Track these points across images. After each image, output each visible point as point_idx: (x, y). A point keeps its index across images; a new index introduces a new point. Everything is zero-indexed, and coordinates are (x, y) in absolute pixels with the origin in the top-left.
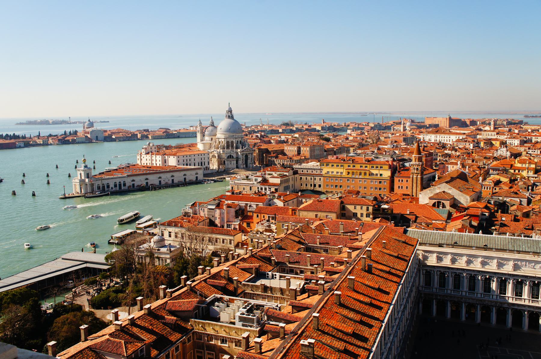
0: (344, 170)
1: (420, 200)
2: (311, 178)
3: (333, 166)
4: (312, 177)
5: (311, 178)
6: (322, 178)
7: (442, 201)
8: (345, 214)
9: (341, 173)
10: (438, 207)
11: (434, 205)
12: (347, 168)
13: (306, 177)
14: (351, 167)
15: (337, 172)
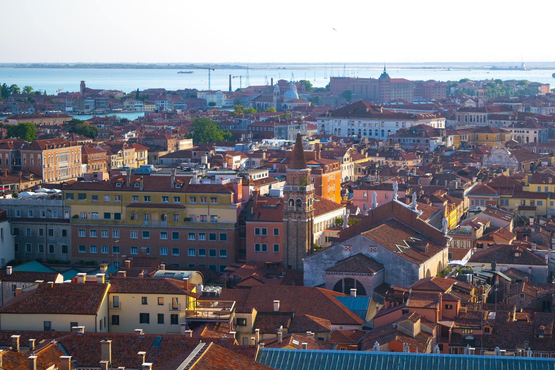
0: (124, 208)
1: (306, 276)
2: (41, 230)
3: (95, 197)
4: (43, 227)
5: (41, 230)
6: (69, 229)
7: (356, 277)
8: (118, 316)
9: (118, 216)
10: (348, 292)
11: (337, 287)
12: (133, 201)
13: (30, 227)
14: (143, 201)
15: (107, 215)
